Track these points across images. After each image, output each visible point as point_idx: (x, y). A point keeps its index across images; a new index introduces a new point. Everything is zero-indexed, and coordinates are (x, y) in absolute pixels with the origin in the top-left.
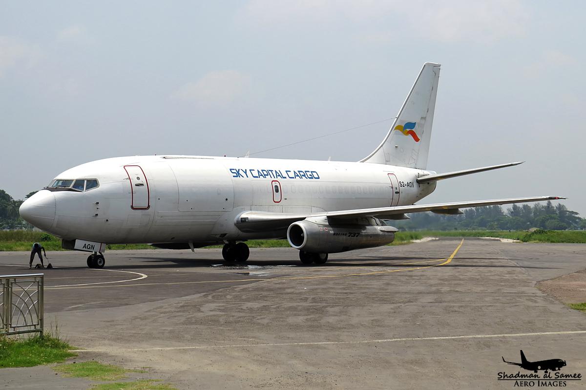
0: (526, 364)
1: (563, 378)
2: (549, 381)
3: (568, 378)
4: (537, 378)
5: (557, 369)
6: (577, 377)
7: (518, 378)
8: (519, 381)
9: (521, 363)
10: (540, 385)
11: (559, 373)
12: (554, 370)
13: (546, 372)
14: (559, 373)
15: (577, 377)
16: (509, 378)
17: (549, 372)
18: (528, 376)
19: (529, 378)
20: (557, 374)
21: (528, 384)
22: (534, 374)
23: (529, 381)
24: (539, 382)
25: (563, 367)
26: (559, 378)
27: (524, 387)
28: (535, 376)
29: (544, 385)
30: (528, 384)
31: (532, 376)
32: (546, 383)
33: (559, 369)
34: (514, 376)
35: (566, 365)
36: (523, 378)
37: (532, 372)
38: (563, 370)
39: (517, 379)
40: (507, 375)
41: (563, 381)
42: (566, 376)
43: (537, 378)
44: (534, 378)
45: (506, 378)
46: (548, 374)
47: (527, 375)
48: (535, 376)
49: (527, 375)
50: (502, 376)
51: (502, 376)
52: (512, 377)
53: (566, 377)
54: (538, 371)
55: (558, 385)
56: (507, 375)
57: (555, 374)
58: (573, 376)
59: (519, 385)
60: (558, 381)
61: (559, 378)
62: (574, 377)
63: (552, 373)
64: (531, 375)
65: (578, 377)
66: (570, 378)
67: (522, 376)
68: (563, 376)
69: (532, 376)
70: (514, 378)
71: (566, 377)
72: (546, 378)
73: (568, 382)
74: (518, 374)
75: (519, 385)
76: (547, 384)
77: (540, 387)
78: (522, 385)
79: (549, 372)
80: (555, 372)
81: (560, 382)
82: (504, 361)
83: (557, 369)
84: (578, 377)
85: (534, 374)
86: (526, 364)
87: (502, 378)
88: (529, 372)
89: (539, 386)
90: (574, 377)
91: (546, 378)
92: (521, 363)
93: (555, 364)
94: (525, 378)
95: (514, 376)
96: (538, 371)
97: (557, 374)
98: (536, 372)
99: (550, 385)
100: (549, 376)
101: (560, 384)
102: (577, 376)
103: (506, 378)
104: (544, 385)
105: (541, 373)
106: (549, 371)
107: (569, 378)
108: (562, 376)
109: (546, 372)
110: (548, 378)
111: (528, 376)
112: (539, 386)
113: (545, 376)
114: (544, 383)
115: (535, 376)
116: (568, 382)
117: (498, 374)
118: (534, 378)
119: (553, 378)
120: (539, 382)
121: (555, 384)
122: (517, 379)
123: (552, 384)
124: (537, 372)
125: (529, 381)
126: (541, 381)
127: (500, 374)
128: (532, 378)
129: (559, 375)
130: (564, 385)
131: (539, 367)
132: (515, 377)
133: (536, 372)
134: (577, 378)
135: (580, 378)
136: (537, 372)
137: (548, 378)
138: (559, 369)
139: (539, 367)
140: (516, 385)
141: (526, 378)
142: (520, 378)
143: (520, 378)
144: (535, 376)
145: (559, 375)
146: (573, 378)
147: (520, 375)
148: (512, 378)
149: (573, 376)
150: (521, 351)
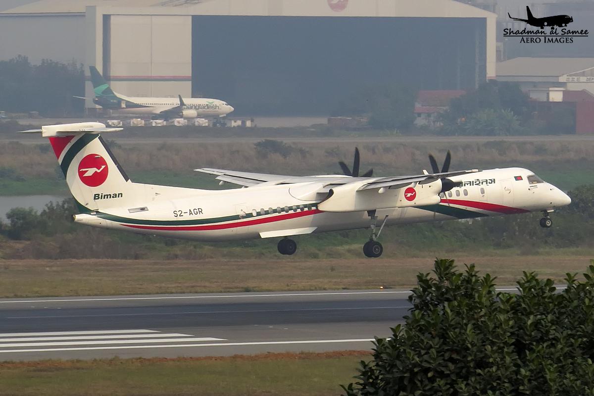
0: (531, 20)
1: (569, 35)
2: (556, 37)
4: (543, 34)
5: (563, 25)
7: (524, 34)
8: (525, 38)
9: (527, 19)
12: (561, 26)
13: (553, 28)
15: (584, 33)
16: (515, 35)
18: (534, 32)
19: (535, 35)
21: (534, 41)
22: (540, 30)
24: (545, 38)
25: (570, 23)
26: (566, 35)
27: (530, 43)
29: (550, 42)
30: (534, 41)
31: (538, 33)
32: (552, 39)
33: (566, 26)
35: (572, 21)
36: (530, 34)
37: (539, 28)
38: (570, 27)
39: (523, 35)
40: (512, 31)
41: (570, 37)
42: (573, 32)
43: (543, 34)
44: (540, 35)
45: (512, 34)
46: (554, 31)
47: (533, 32)
53: (573, 34)
54: (545, 27)
56: (512, 31)
58: (579, 32)
59: (525, 40)
60: (565, 37)
61: (566, 35)
62: (581, 33)
63: (559, 30)
64: (538, 32)
65: (585, 33)
66: (577, 34)
67: (528, 32)
68: (569, 32)
70: (520, 35)
71: (573, 34)
72: (552, 35)
74: (524, 31)
75: (525, 40)
76: (554, 41)
78: (528, 41)
80: (562, 28)
81: (566, 38)
82: (510, 17)
83: (563, 25)
84: (585, 33)
85: (540, 30)
86: (531, 20)
87: (508, 35)
88: (535, 28)
89: (545, 42)
90: (581, 33)
91: (552, 35)
92: (527, 19)
93: (562, 20)
94: (531, 35)
96: (545, 27)
97: (564, 30)
98: (542, 28)
99: (556, 42)
100: (556, 32)
101: (566, 40)
102: (584, 32)
103: (512, 34)
104: (550, 42)
105: (547, 29)
106: (555, 27)
107: (576, 35)
109: (553, 28)
110: (555, 35)
111: (534, 32)
112: (545, 42)
113: (552, 33)
114: (550, 40)
118: (540, 35)
119: (560, 34)
120: (545, 38)
121: (562, 40)
122: (523, 35)
123: (559, 41)
125: (535, 38)
126: (547, 38)
128: (538, 35)
129: (566, 31)
130: (571, 42)
131: (546, 24)
132: (521, 33)
133: (542, 28)
134: (584, 35)
137: (555, 35)
138: (566, 26)
139: (546, 24)
140: (523, 42)
141: (532, 34)
142: (527, 35)
143: (527, 35)
144: (542, 32)
145: (566, 31)
146: (580, 35)
148: (518, 35)
149: (579, 32)
150: (527, 7)
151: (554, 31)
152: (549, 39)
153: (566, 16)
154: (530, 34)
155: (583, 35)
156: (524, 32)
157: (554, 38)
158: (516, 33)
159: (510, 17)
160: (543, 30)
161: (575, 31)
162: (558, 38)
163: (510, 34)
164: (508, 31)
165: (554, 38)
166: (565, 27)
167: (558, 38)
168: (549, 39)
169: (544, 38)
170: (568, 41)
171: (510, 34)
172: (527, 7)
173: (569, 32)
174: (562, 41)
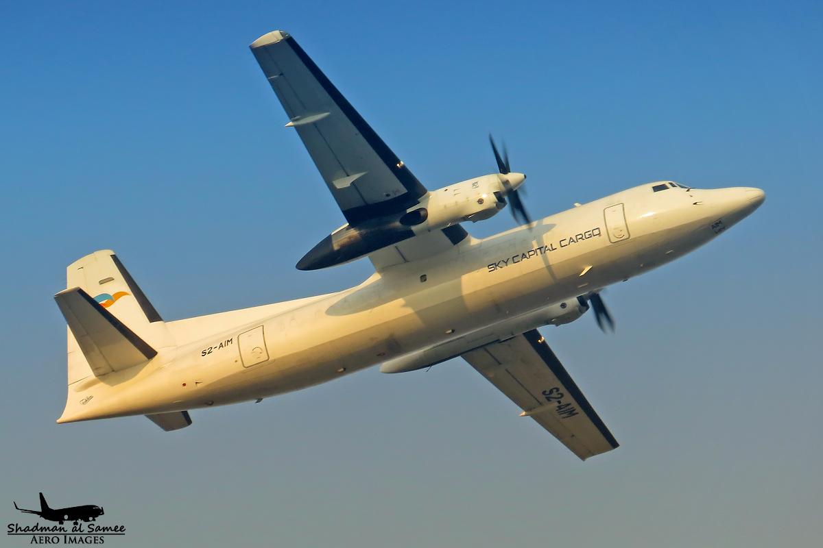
0: (47, 513)
3: (106, 532)
4: (62, 532)
5: (91, 519)
6: (119, 530)
7: (36, 532)
8: (37, 537)
9: (40, 511)
10: (67, 542)
11: (93, 525)
12: (87, 520)
13: (76, 523)
14: (93, 525)
15: (119, 530)
16: (23, 532)
17: (79, 524)
19: (51, 532)
20: (91, 526)
21: (50, 541)
22: (59, 526)
23: (51, 537)
25: (100, 516)
26: (94, 532)
28: (60, 529)
29: (72, 542)
30: (50, 541)
31: (56, 529)
32: (75, 539)
33: (94, 520)
34: (30, 529)
35: (103, 513)
36: (44, 532)
37: (57, 523)
38: (100, 521)
39: (34, 533)
40: (20, 528)
41: (99, 536)
43: (62, 532)
45: (19, 532)
46: (78, 527)
47: (48, 528)
48: (60, 529)
49: (48, 528)
50: (14, 530)
51: (14, 530)
52: (28, 530)
54: (65, 522)
55: (93, 542)
56: (20, 528)
57: (89, 526)
58: (113, 528)
59: (38, 541)
60: (93, 536)
61: (94, 532)
62: (115, 530)
63: (84, 525)
64: (55, 528)
65: (120, 530)
66: (110, 532)
67: (42, 529)
68: (99, 529)
69: (56, 529)
70: (31, 532)
72: (75, 532)
73: (106, 538)
74: (37, 527)
75: (38, 541)
76: (77, 541)
77: (67, 544)
78: (42, 542)
79: (79, 524)
80: (89, 523)
81: (95, 538)
82: (17, 508)
83: (91, 519)
84: (120, 530)
85: (59, 526)
86: (47, 513)
87: (14, 532)
88: (51, 524)
89: (65, 542)
90: (115, 530)
91: (75, 532)
92: (40, 511)
93: (89, 512)
94: (45, 533)
95: (30, 529)
97: (91, 526)
98: (61, 523)
99: (81, 542)
100: (80, 529)
101: (95, 540)
102: (119, 529)
103: (19, 532)
104: (72, 542)
105: (68, 525)
106: (79, 521)
108: (98, 528)
109: (76, 523)
110: (79, 532)
112: (65, 542)
113: (74, 530)
114: (73, 539)
115: (60, 529)
116: (106, 538)
117: (9, 526)
118: (58, 532)
119: (86, 532)
121: (88, 540)
122: (34, 533)
123: (84, 541)
124: (62, 523)
125: (51, 537)
126: (68, 537)
127: (11, 526)
128: (56, 532)
129: (94, 527)
130: (101, 542)
131: (66, 517)
132: (32, 530)
133: (61, 523)
134: (119, 532)
135: (123, 533)
136: (62, 523)
137: (79, 532)
138: (94, 520)
139: (66, 517)
140: (34, 542)
141: (48, 532)
142: (40, 532)
143: (40, 532)
144: (60, 529)
145: (94, 527)
146: (114, 532)
147: (39, 528)
148: (28, 532)
150: (41, 494)
151: (78, 527)
152: (70, 538)
153: (95, 506)
154: (44, 532)
155: (118, 533)
156: (37, 528)
157: (78, 538)
158: (24, 530)
159: (17, 508)
160: (62, 526)
161: (107, 528)
162: (84, 537)
163: (16, 531)
164: (14, 528)
165: (78, 538)
166: (93, 522)
167: (84, 537)
168: (70, 538)
169: (63, 536)
170: (96, 541)
171: (16, 531)
172: (41, 494)
173: (99, 529)
174: (88, 541)
